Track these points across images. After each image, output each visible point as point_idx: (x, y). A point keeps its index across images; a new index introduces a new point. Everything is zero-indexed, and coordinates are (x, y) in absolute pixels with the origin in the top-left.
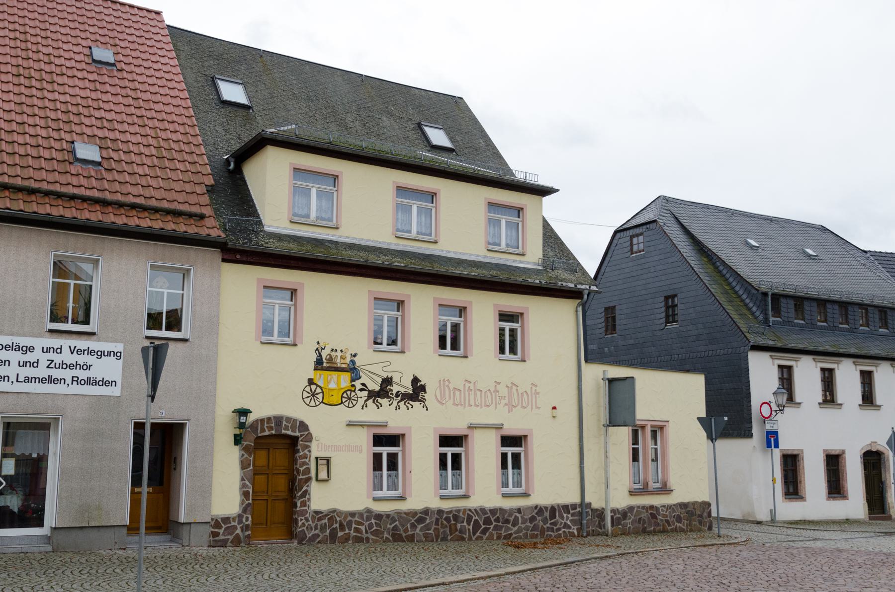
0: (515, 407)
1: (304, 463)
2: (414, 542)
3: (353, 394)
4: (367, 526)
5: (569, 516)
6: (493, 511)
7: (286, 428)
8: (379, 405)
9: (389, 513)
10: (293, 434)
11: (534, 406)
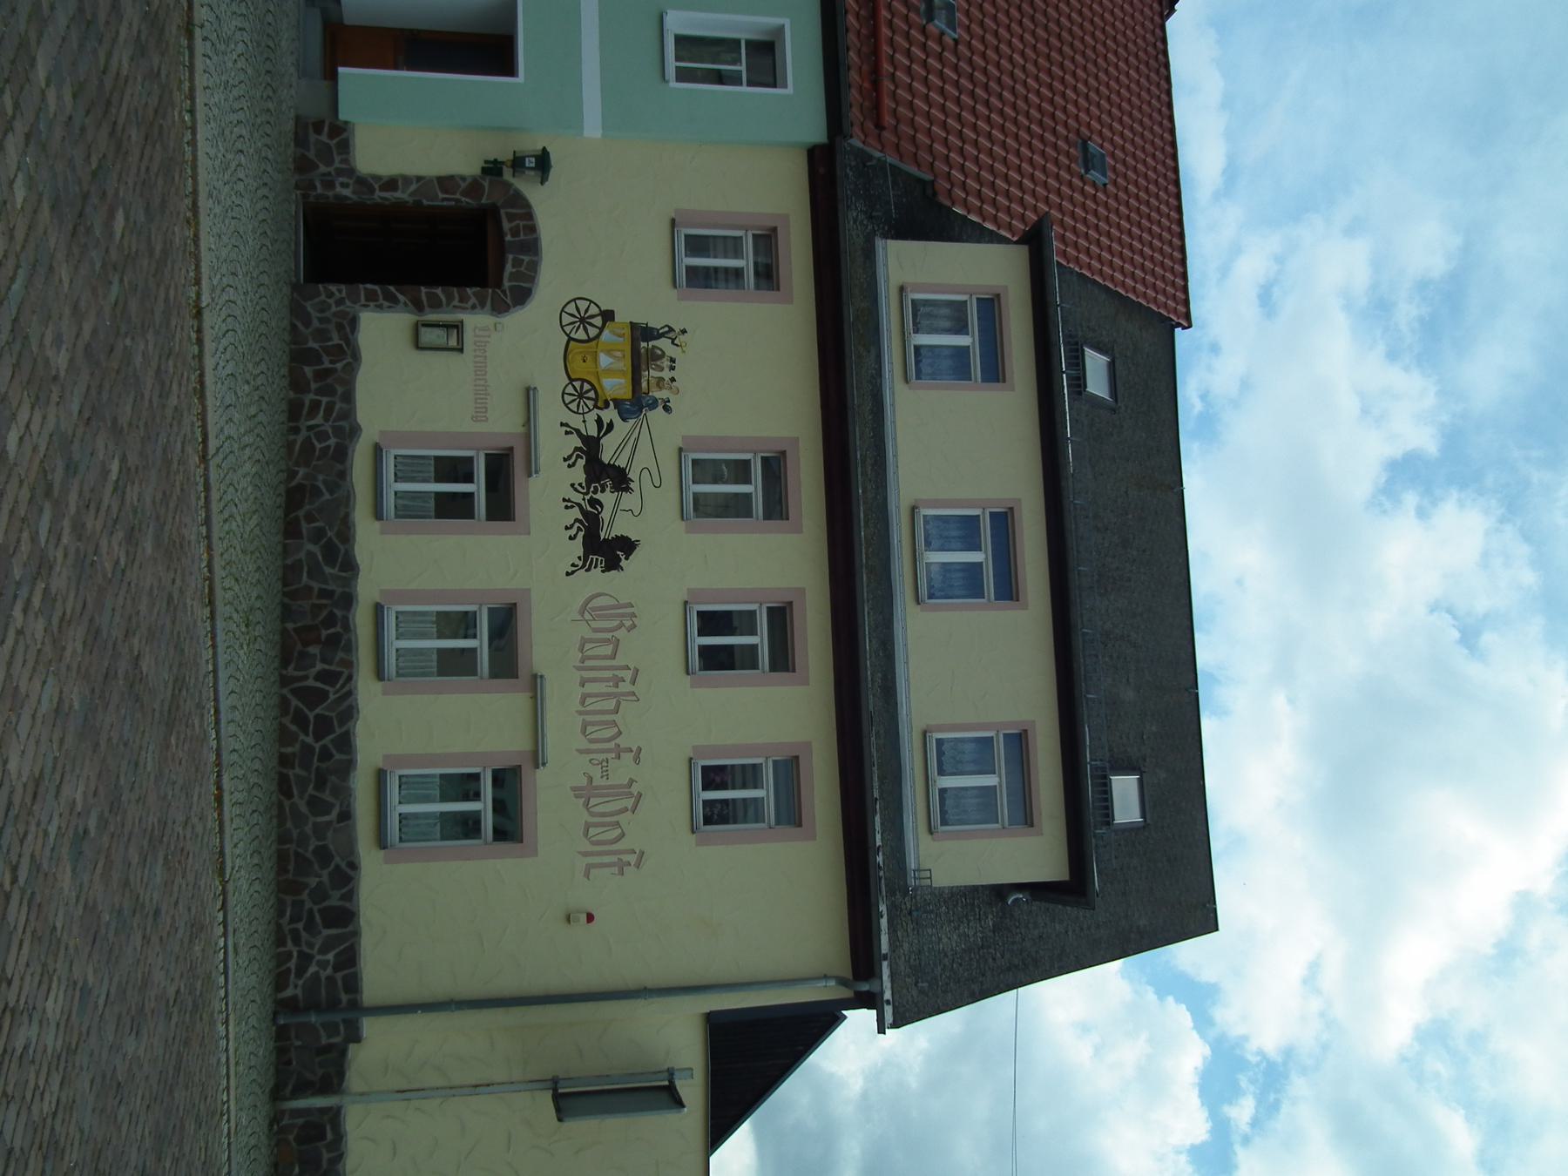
0: (586, 804)
1: (450, 298)
2: (286, 538)
3: (590, 404)
4: (323, 428)
5: (329, 971)
6: (346, 743)
7: (517, 263)
8: (571, 462)
9: (348, 478)
10: (506, 274)
11: (590, 860)
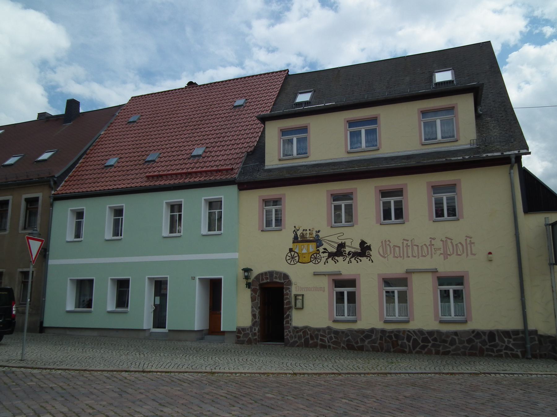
0: (450, 255)
1: (287, 298)
3: (318, 255)
5: (511, 340)
6: (431, 333)
7: (276, 278)
8: (336, 261)
10: (279, 281)
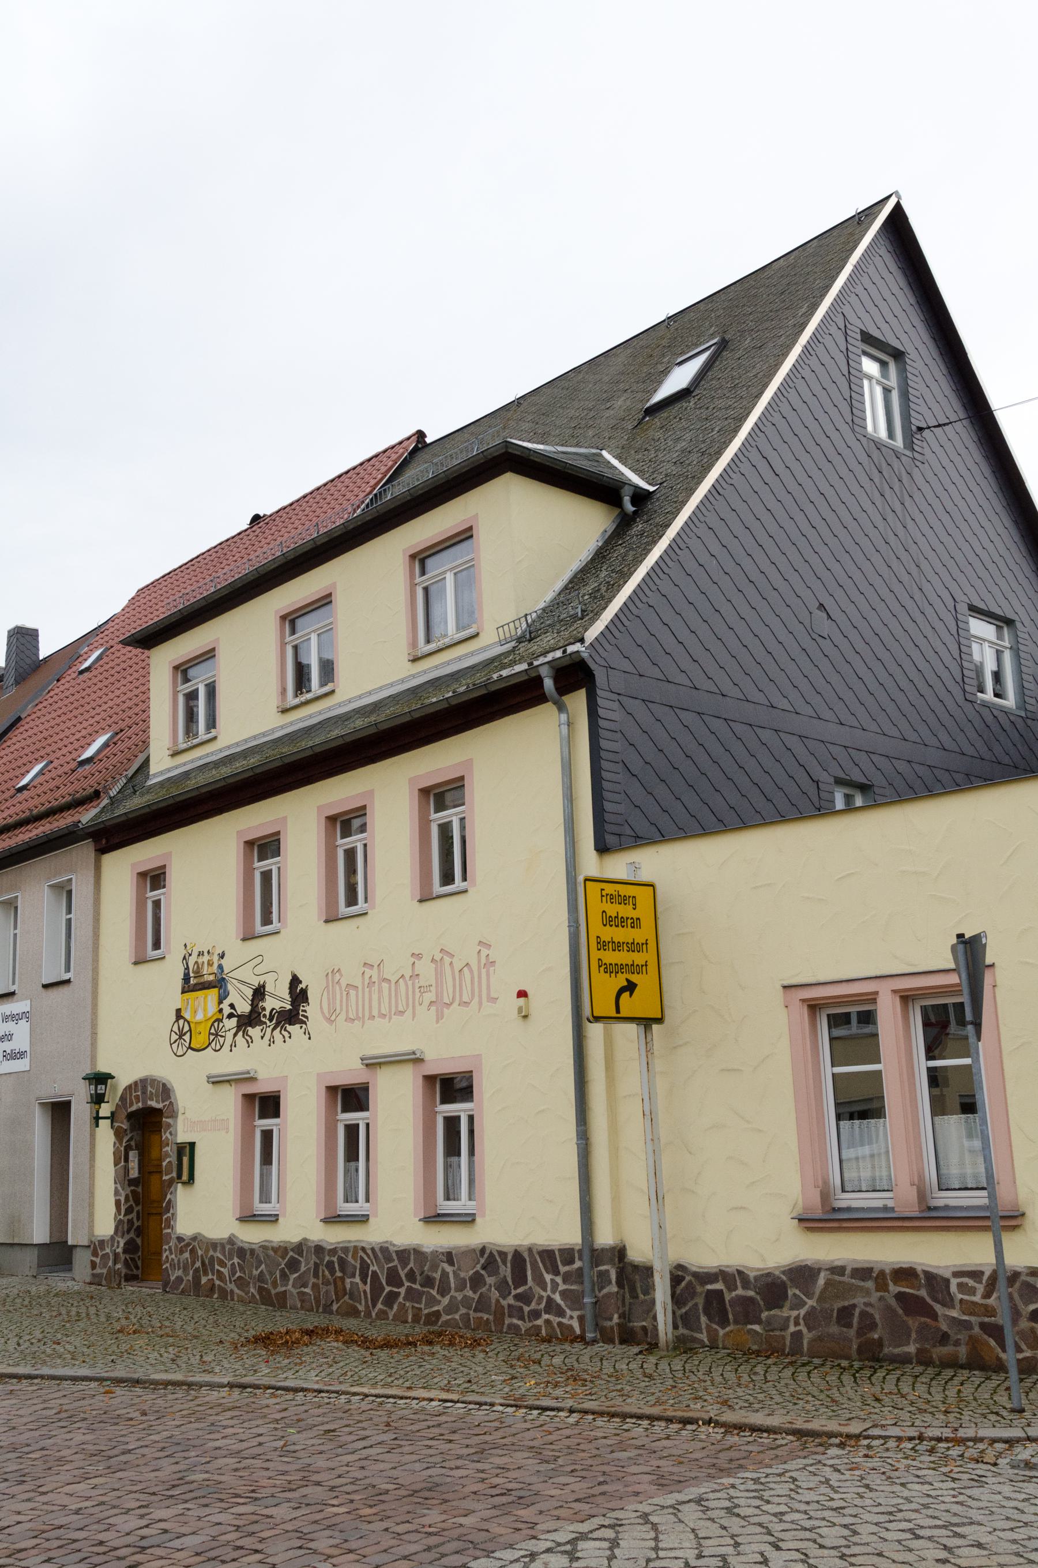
0: (448, 1005)
5: (559, 1279)
6: (403, 1255)
8: (250, 1041)
